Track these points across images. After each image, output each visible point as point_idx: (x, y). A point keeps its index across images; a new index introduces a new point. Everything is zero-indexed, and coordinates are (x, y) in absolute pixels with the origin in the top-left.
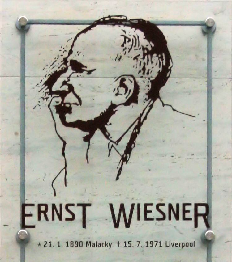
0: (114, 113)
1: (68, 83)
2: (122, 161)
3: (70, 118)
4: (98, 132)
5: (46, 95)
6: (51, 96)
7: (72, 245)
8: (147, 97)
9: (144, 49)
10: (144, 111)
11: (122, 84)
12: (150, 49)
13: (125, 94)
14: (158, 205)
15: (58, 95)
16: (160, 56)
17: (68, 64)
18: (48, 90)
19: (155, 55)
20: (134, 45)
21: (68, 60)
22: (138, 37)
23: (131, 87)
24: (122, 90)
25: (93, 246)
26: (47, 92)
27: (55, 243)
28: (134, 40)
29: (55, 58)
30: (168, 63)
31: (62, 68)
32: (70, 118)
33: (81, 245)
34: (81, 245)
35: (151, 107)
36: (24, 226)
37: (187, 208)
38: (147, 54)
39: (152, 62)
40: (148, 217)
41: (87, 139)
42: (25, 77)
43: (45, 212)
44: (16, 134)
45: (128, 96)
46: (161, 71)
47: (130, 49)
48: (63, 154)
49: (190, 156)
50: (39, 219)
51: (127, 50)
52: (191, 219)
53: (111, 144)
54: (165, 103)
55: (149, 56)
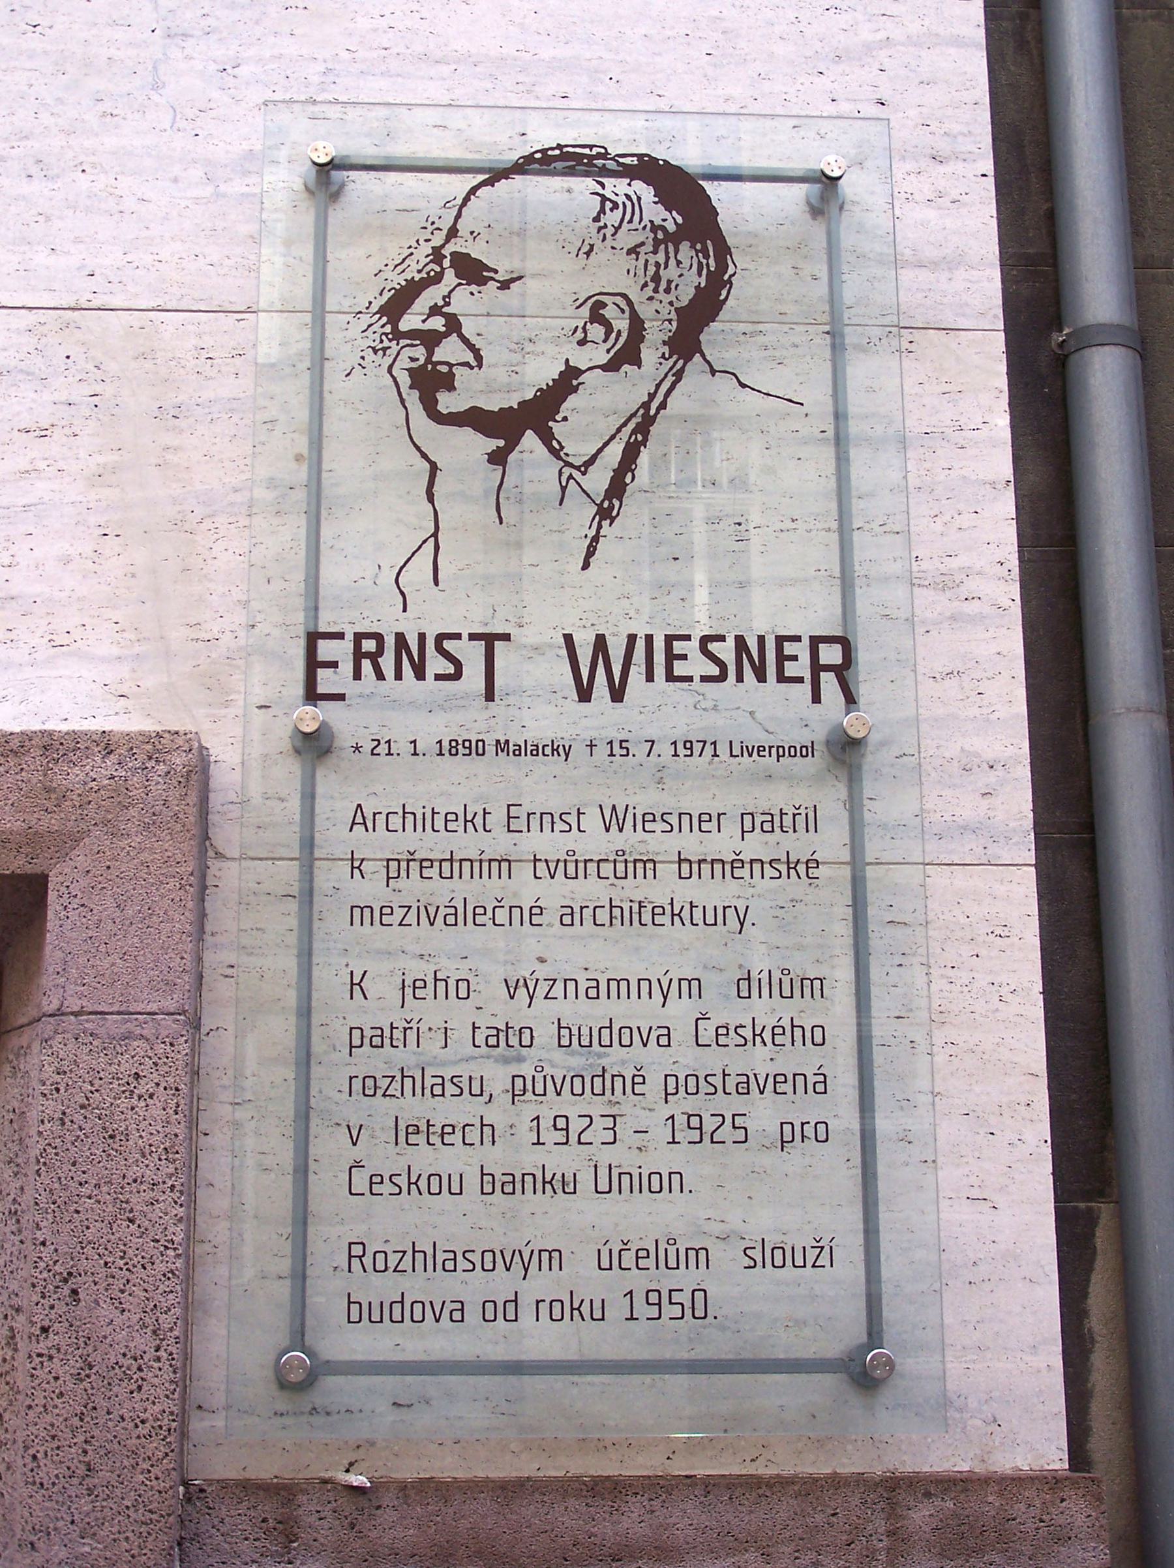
0: (575, 390)
1: (445, 310)
2: (597, 518)
3: (447, 402)
4: (530, 439)
5: (382, 341)
6: (398, 344)
7: (454, 751)
8: (666, 350)
9: (655, 228)
10: (658, 386)
11: (596, 316)
12: (671, 227)
13: (604, 341)
14: (705, 640)
15: (418, 342)
16: (699, 247)
17: (446, 263)
18: (388, 329)
19: (685, 246)
20: (627, 217)
21: (446, 252)
22: (639, 199)
23: (621, 324)
24: (597, 331)
25: (517, 753)
26: (386, 334)
27: (402, 746)
28: (628, 204)
29: (410, 247)
30: (722, 266)
31: (428, 273)
32: (447, 402)
33: (480, 751)
34: (480, 751)
35: (679, 376)
36: (312, 695)
37: (789, 649)
38: (664, 241)
39: (679, 263)
40: (675, 662)
41: (498, 458)
42: (324, 312)
43: (374, 657)
44: (298, 458)
45: (613, 346)
46: (703, 285)
47: (617, 229)
48: (431, 498)
49: (789, 524)
50: (357, 675)
51: (609, 231)
52: (800, 680)
53: (567, 471)
54: (715, 368)
55: (670, 246)
